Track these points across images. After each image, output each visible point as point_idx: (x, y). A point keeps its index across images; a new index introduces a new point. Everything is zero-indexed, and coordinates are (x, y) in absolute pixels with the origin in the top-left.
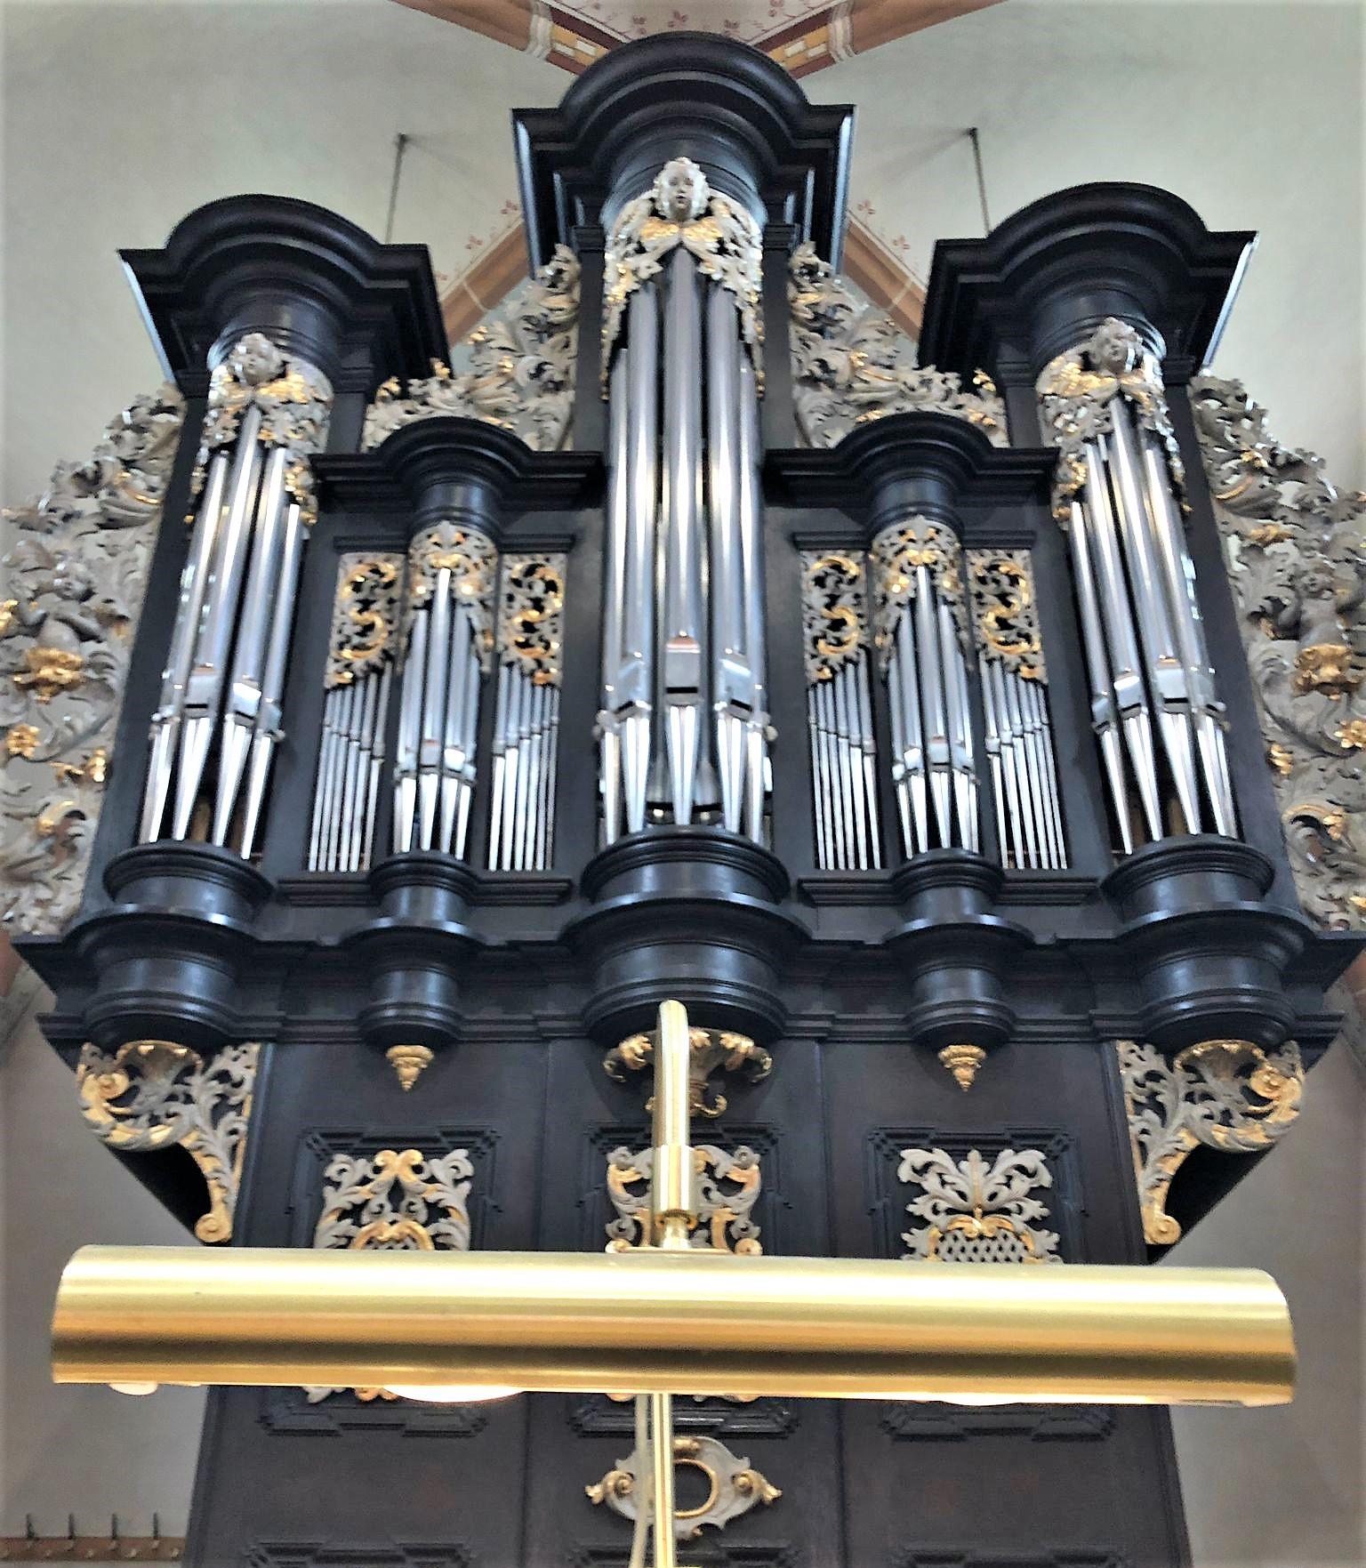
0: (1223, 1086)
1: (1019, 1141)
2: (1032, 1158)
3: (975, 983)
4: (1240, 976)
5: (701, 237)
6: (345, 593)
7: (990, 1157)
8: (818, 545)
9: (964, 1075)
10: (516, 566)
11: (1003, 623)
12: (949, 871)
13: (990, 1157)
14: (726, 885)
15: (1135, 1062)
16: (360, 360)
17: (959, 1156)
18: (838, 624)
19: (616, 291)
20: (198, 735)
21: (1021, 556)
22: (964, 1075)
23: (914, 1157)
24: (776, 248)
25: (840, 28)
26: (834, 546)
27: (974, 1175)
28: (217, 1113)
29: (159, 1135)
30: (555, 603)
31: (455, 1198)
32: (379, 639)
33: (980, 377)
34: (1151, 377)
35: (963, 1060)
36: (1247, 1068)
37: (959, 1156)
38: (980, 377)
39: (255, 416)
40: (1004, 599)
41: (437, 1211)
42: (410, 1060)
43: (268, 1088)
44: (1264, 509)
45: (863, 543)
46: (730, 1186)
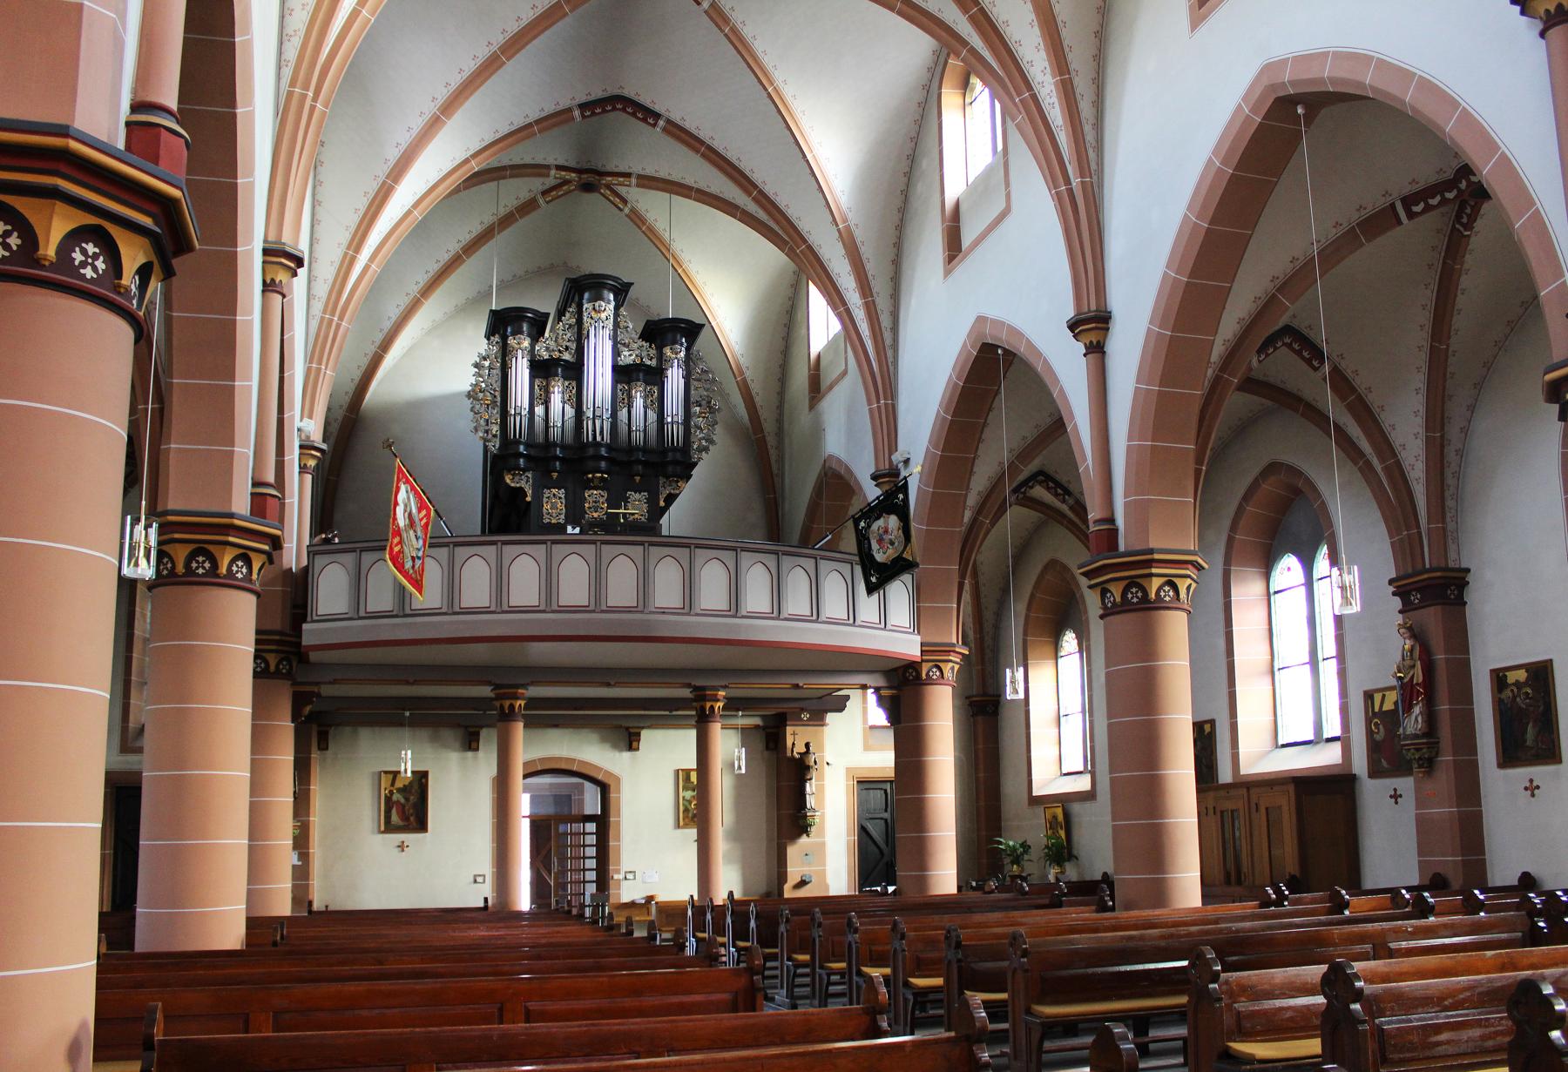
0: (674, 484)
1: (644, 491)
2: (646, 494)
3: (640, 467)
4: (678, 469)
5: (603, 315)
6: (536, 387)
7: (640, 493)
8: (621, 383)
9: (637, 481)
10: (567, 383)
11: (651, 401)
12: (637, 448)
13: (640, 493)
14: (603, 452)
15: (662, 480)
16: (535, 332)
17: (635, 493)
18: (623, 399)
19: (586, 325)
20: (518, 419)
21: (656, 387)
22: (637, 481)
23: (630, 493)
24: (617, 308)
25: (634, 181)
26: (624, 383)
27: (637, 496)
28: (527, 481)
29: (518, 485)
30: (574, 391)
31: (563, 496)
32: (543, 397)
33: (653, 346)
34: (682, 354)
35: (638, 479)
36: (678, 482)
37: (635, 493)
38: (653, 346)
39: (520, 351)
40: (652, 395)
41: (560, 498)
42: (555, 475)
43: (534, 479)
44: (699, 380)
45: (628, 383)
46: (603, 496)
